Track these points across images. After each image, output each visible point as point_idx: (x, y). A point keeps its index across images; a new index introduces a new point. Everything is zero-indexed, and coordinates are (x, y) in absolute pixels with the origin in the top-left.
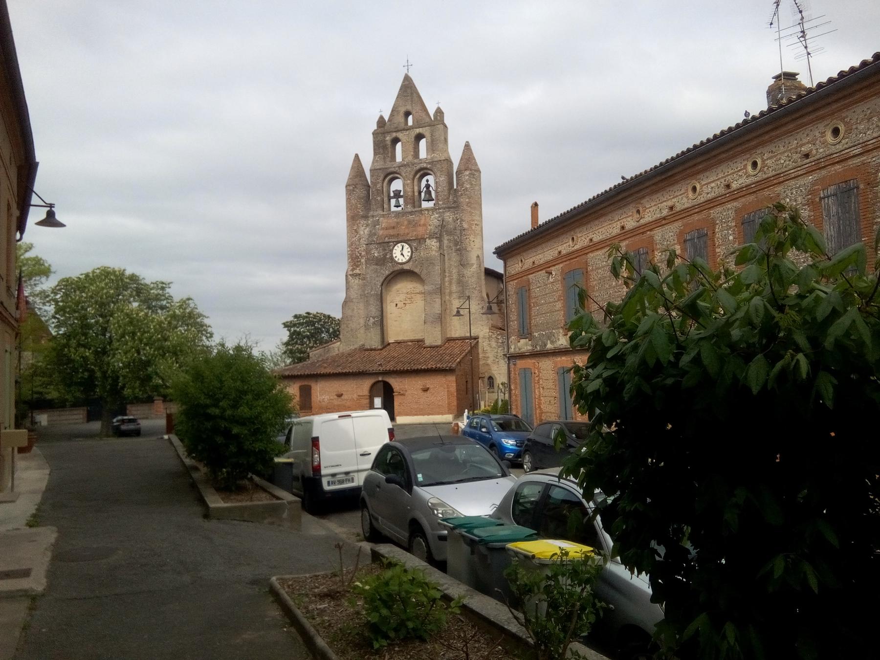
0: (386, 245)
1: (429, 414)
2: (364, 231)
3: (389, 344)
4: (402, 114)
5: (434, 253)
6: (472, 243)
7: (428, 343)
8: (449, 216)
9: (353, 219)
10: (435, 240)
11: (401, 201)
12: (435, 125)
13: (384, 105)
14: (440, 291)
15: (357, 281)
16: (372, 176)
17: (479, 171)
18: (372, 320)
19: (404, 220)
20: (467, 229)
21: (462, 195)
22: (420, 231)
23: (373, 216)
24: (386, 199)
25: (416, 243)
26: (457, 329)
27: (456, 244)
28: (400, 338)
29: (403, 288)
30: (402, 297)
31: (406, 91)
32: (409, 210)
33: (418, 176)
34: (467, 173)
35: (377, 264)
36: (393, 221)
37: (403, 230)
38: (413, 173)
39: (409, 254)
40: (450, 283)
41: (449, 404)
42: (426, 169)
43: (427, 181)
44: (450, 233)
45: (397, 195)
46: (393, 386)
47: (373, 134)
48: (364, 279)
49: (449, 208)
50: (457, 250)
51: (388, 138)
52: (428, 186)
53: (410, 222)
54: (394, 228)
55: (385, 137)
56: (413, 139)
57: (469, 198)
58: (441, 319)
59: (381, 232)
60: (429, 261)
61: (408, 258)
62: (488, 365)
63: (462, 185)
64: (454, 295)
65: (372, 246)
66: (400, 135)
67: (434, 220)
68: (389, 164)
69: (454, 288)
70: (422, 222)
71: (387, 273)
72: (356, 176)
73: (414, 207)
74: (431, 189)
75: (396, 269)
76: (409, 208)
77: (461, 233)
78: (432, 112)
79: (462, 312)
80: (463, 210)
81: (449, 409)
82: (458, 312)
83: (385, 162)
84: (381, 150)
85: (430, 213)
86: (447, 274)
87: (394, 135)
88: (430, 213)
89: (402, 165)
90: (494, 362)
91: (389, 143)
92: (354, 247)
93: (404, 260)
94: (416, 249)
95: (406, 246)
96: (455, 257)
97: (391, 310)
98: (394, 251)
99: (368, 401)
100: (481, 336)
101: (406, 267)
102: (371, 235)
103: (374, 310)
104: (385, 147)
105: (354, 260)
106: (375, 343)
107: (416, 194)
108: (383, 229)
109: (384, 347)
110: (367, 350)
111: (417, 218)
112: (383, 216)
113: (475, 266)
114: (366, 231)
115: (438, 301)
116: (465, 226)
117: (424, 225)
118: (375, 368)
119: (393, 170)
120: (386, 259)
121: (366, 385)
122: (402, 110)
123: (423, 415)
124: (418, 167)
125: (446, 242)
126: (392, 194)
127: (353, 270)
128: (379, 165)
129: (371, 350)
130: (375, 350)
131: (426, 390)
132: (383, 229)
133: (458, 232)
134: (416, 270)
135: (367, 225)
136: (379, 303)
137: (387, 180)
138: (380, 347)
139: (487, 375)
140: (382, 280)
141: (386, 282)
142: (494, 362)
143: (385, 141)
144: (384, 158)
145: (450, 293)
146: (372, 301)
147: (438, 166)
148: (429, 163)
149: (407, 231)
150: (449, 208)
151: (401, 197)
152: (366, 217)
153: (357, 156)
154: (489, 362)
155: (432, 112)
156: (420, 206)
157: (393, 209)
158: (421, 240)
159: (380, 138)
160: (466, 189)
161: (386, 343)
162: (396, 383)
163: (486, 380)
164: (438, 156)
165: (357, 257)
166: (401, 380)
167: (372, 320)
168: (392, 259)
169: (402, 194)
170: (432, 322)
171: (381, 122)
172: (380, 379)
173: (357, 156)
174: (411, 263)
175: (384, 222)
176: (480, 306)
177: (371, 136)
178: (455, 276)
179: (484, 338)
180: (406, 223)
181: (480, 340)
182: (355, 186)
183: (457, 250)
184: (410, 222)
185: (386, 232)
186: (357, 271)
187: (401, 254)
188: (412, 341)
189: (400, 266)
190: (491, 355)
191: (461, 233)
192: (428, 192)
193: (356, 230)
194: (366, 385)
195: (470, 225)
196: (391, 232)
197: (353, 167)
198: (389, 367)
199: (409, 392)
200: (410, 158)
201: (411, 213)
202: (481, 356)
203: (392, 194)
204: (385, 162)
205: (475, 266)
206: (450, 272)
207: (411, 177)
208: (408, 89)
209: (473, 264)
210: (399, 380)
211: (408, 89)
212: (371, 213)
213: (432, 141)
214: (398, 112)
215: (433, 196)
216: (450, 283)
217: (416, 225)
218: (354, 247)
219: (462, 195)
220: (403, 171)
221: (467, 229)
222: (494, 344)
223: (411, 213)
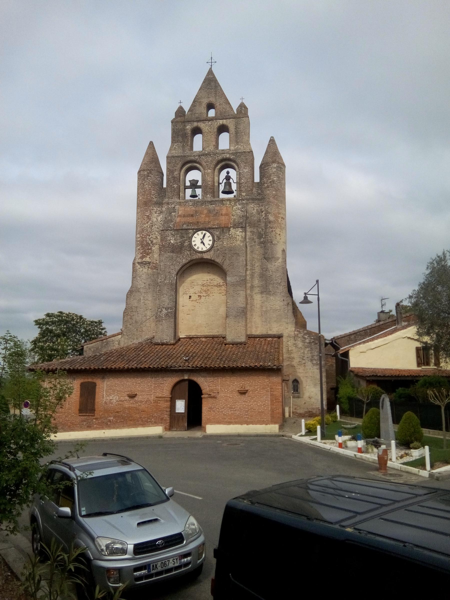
0: (186, 232)
1: (248, 423)
2: (157, 218)
3: (179, 339)
4: (204, 105)
5: (238, 242)
6: (278, 237)
7: (229, 339)
8: (253, 208)
9: (144, 204)
10: (240, 230)
11: (199, 192)
12: (236, 121)
13: (186, 94)
14: (243, 282)
15: (145, 270)
16: (168, 163)
17: (284, 165)
18: (164, 311)
19: (204, 209)
20: (274, 222)
21: (268, 187)
22: (223, 220)
23: (168, 204)
24: (182, 187)
25: (219, 231)
26: (258, 328)
27: (260, 236)
28: (193, 333)
29: (200, 279)
30: (197, 289)
31: (209, 84)
32: (209, 200)
33: (219, 167)
34: (275, 165)
35: (173, 252)
36: (190, 209)
37: (203, 218)
38: (214, 162)
39: (211, 243)
40: (252, 276)
41: (272, 411)
42: (229, 159)
43: (228, 173)
44: (253, 225)
45: (194, 185)
46: (202, 388)
47: (172, 122)
48: (156, 268)
49: (253, 199)
50: (261, 243)
51: (189, 127)
52: (228, 178)
53: (210, 211)
54: (192, 216)
55: (185, 126)
56: (216, 130)
57: (276, 191)
58: (243, 313)
59: (178, 220)
60: (233, 252)
61: (208, 247)
62: (293, 366)
63: (269, 177)
64: (257, 290)
65: (169, 233)
66: (202, 125)
67: (237, 211)
68: (188, 153)
69: (256, 282)
70: (224, 212)
71: (184, 261)
72: (151, 162)
73: (214, 197)
74: (231, 181)
75: (195, 257)
76: (209, 197)
77: (266, 226)
78: (235, 106)
79: (310, 298)
80: (269, 202)
81: (273, 417)
82: (306, 298)
83: (184, 151)
84: (180, 139)
85: (233, 203)
86: (249, 267)
87: (195, 124)
88: (233, 203)
89: (201, 155)
90: (300, 363)
91: (189, 132)
92: (145, 233)
93: (205, 249)
94: (219, 238)
95: (208, 234)
96: (258, 250)
97: (183, 300)
98: (193, 239)
99: (169, 403)
100: (285, 335)
101: (206, 256)
102: (166, 221)
103: (166, 301)
104: (184, 136)
105: (144, 246)
106: (168, 338)
107: (216, 184)
108: (180, 216)
109: (176, 342)
110: (158, 344)
111: (218, 208)
112: (180, 204)
113: (280, 260)
114: (159, 219)
115: (242, 293)
116: (271, 218)
117: (227, 215)
118: (180, 363)
119: (193, 158)
120: (185, 246)
121: (167, 384)
122: (205, 101)
123: (241, 423)
124: (220, 157)
125: (248, 234)
126: (188, 184)
127: (142, 258)
128: (178, 152)
129: (163, 344)
130: (167, 344)
131: (243, 393)
132: (180, 216)
133: (263, 225)
134: (218, 260)
135: (161, 212)
136: (173, 293)
137: (184, 168)
138: (172, 342)
139: (291, 378)
140: (178, 268)
141: (181, 272)
142: (300, 363)
143: (185, 130)
144: (183, 147)
145: (252, 287)
146: (165, 290)
147: (242, 157)
148: (233, 154)
149: (207, 219)
150: (253, 199)
151: (199, 187)
152: (160, 204)
153: (151, 143)
154: (295, 363)
155: (235, 106)
156: (219, 197)
157: (188, 197)
158: (224, 229)
159: (180, 126)
160: (273, 181)
161: (177, 338)
162: (206, 383)
163: (290, 383)
164: (241, 148)
165: (148, 244)
166: (211, 379)
167: (164, 311)
168: (190, 246)
169: (200, 183)
170: (236, 317)
171: (180, 112)
172: (186, 378)
173: (151, 143)
174: (212, 252)
175: (181, 210)
176: (286, 303)
177: (170, 124)
178: (257, 270)
179: (289, 336)
180: (205, 212)
181: (284, 339)
182: (150, 172)
183: (261, 243)
184: (210, 211)
185: (183, 220)
186: (147, 259)
187: (201, 242)
188: (206, 337)
189: (199, 255)
190: (296, 356)
191: (266, 226)
192: (228, 184)
193: (148, 216)
194: (167, 384)
195: (276, 217)
196: (190, 220)
197: (147, 153)
198: (198, 363)
199: (222, 394)
200: (211, 148)
201: (211, 202)
202: (285, 356)
203: (188, 184)
204: (184, 151)
205: (280, 260)
206: (253, 265)
207: (212, 166)
208: (211, 82)
209: (278, 259)
210: (210, 379)
211: (211, 82)
212: (166, 200)
213: (237, 133)
214: (200, 103)
215: (234, 187)
216: (252, 276)
217: (217, 214)
218: (145, 233)
219: (268, 187)
220: (203, 160)
221: (274, 222)
222: (300, 344)
223: (211, 202)
